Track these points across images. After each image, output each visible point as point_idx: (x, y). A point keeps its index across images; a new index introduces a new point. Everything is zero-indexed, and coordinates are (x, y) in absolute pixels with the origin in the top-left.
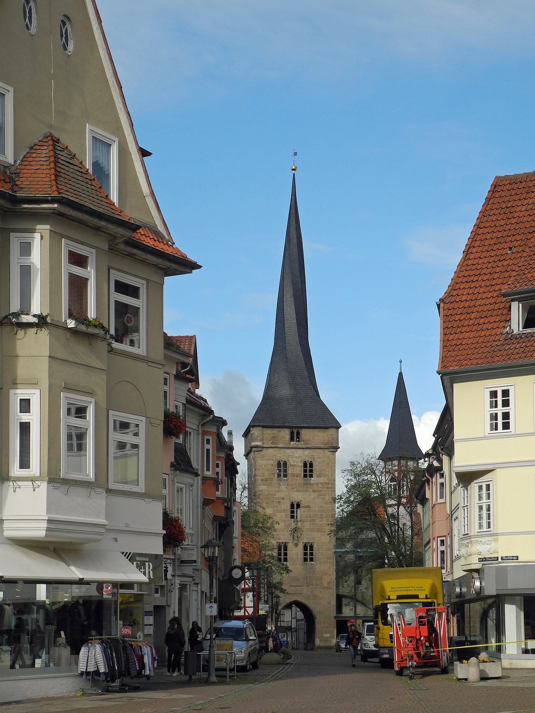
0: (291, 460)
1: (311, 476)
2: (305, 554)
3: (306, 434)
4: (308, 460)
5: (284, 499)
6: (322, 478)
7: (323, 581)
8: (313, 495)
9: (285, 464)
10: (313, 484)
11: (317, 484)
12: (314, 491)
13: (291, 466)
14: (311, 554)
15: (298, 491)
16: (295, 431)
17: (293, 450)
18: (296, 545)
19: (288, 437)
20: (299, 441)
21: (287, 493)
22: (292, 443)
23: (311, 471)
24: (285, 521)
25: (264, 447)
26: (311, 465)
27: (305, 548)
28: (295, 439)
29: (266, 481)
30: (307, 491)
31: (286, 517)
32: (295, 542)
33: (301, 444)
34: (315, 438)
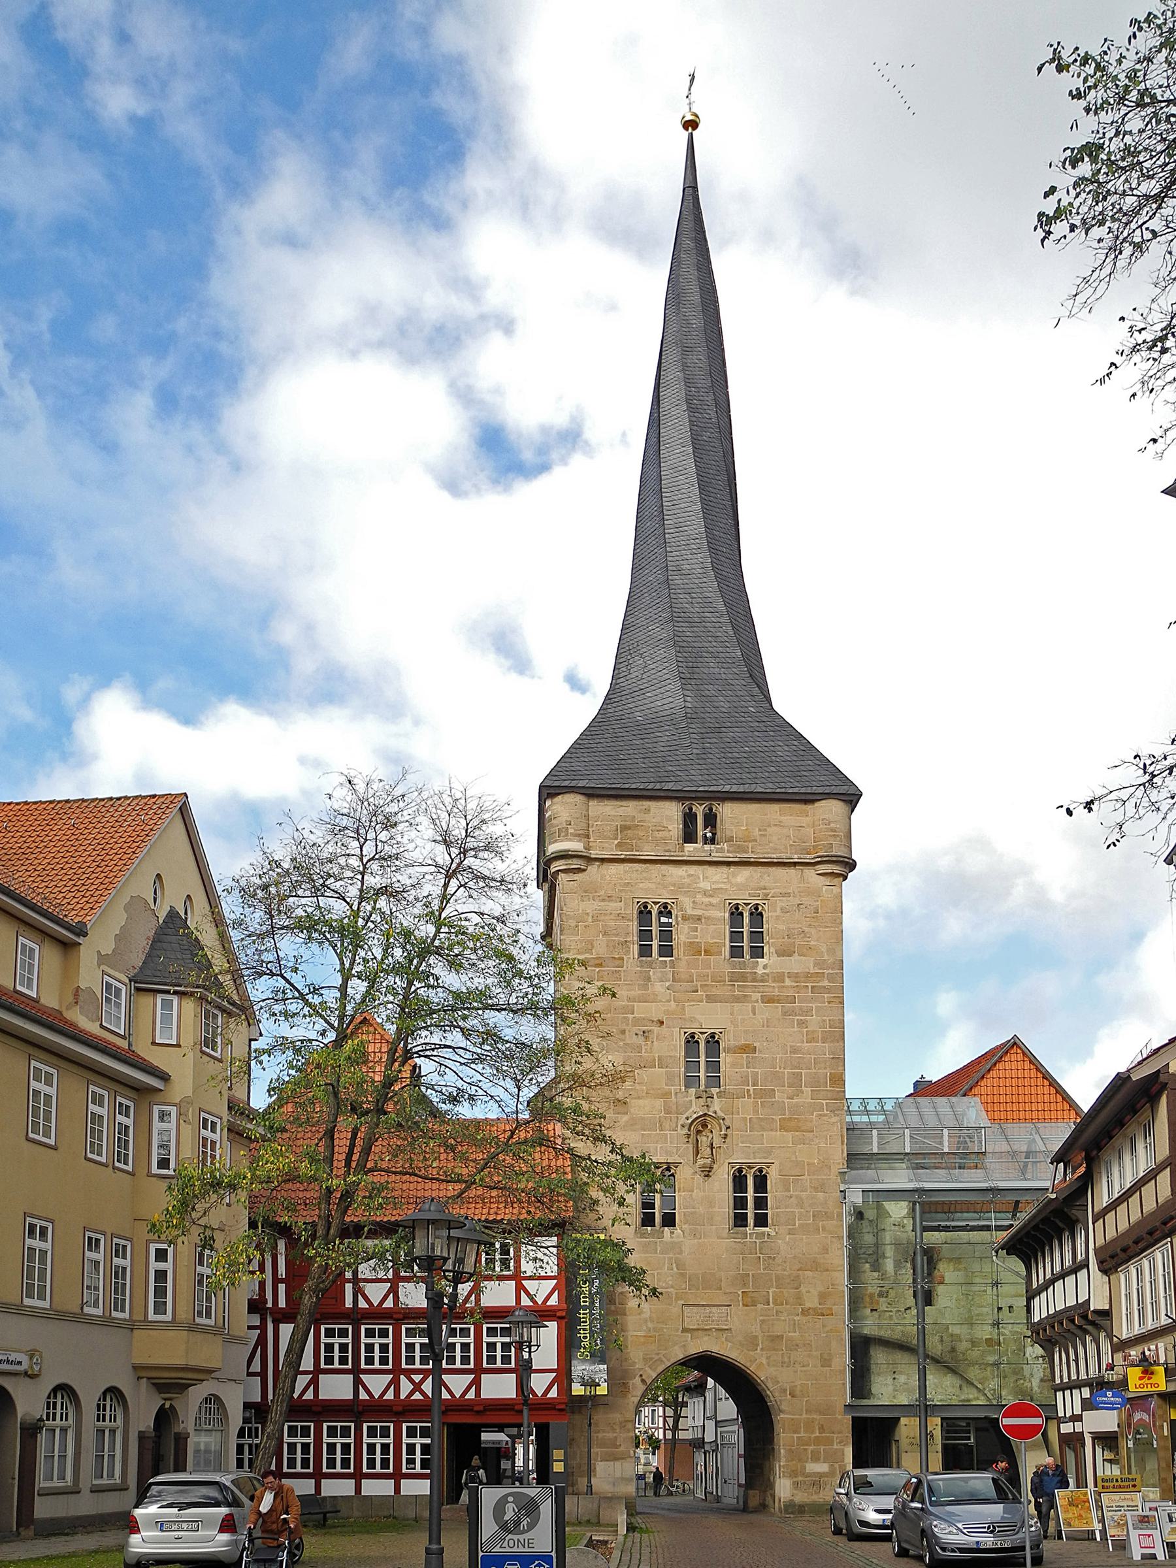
0: (686, 901)
1: (758, 953)
2: (740, 1203)
4: (744, 899)
7: (803, 1289)
8: (765, 1012)
9: (665, 911)
11: (780, 978)
13: (685, 918)
14: (761, 1203)
15: (710, 999)
16: (700, 810)
17: (693, 869)
18: (707, 1172)
19: (676, 828)
20: (713, 841)
22: (689, 847)
23: (757, 936)
24: (667, 1094)
25: (589, 860)
26: (757, 915)
27: (739, 1182)
28: (700, 833)
29: (600, 965)
30: (744, 999)
31: (670, 1079)
32: (701, 1162)
33: (721, 850)
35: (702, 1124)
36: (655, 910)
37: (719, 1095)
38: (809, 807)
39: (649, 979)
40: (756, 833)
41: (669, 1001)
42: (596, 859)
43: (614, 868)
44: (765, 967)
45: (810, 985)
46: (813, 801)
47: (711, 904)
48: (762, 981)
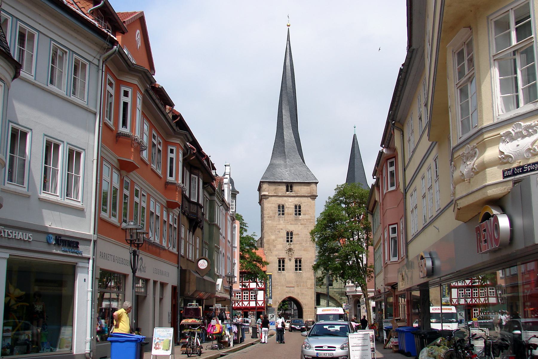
0: (287, 204)
2: (296, 266)
4: (298, 203)
8: (301, 227)
9: (283, 206)
10: (300, 220)
11: (304, 220)
12: (301, 224)
14: (300, 266)
15: (291, 224)
18: (290, 260)
23: (300, 211)
24: (283, 244)
26: (300, 207)
27: (296, 262)
30: (297, 224)
31: (284, 241)
35: (290, 250)
43: (273, 198)
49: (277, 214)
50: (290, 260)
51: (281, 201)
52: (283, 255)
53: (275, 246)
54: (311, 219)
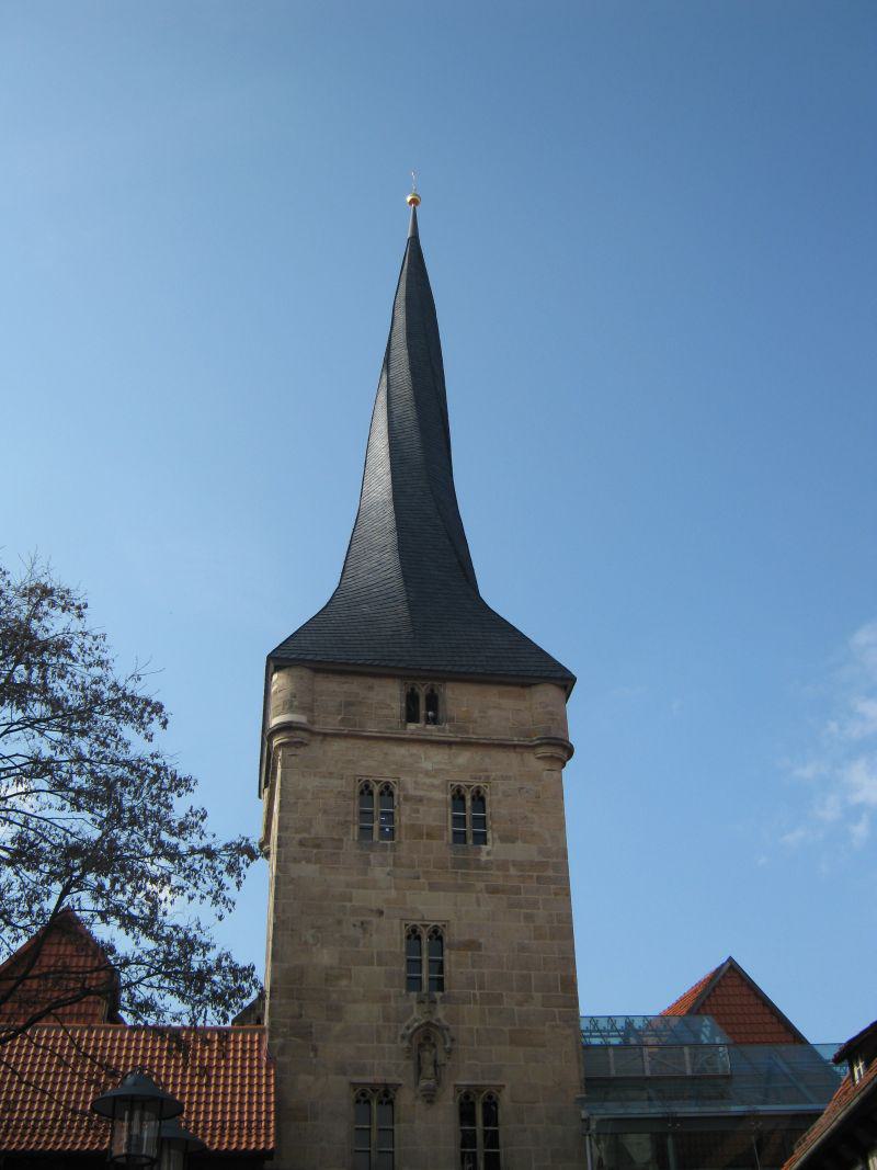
0: (407, 780)
1: (481, 839)
3: (460, 700)
4: (463, 779)
5: (381, 913)
6: (519, 844)
9: (387, 791)
10: (487, 866)
11: (503, 866)
12: (493, 890)
13: (407, 798)
15: (433, 887)
16: (422, 692)
17: (415, 749)
18: (430, 1097)
19: (397, 707)
20: (434, 720)
21: (393, 893)
22: (412, 726)
23: (481, 822)
24: (385, 998)
25: (313, 733)
26: (479, 799)
27: (466, 1114)
28: (422, 712)
29: (318, 846)
32: (423, 1083)
33: (443, 730)
34: (491, 712)
36: (376, 789)
37: (444, 1000)
38: (527, 691)
39: (368, 863)
40: (476, 714)
41: (389, 888)
42: (319, 734)
44: (488, 853)
45: (535, 874)
46: (530, 685)
47: (433, 786)
48: (486, 869)
49: (355, 829)
50: (430, 1097)
51: (377, 762)
52: (387, 1063)
53: (335, 1012)
54: (543, 865)
